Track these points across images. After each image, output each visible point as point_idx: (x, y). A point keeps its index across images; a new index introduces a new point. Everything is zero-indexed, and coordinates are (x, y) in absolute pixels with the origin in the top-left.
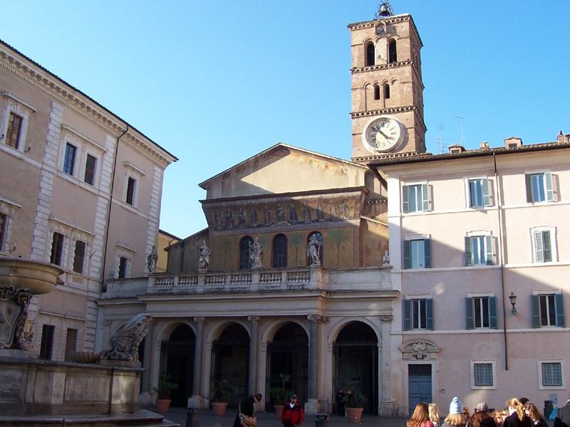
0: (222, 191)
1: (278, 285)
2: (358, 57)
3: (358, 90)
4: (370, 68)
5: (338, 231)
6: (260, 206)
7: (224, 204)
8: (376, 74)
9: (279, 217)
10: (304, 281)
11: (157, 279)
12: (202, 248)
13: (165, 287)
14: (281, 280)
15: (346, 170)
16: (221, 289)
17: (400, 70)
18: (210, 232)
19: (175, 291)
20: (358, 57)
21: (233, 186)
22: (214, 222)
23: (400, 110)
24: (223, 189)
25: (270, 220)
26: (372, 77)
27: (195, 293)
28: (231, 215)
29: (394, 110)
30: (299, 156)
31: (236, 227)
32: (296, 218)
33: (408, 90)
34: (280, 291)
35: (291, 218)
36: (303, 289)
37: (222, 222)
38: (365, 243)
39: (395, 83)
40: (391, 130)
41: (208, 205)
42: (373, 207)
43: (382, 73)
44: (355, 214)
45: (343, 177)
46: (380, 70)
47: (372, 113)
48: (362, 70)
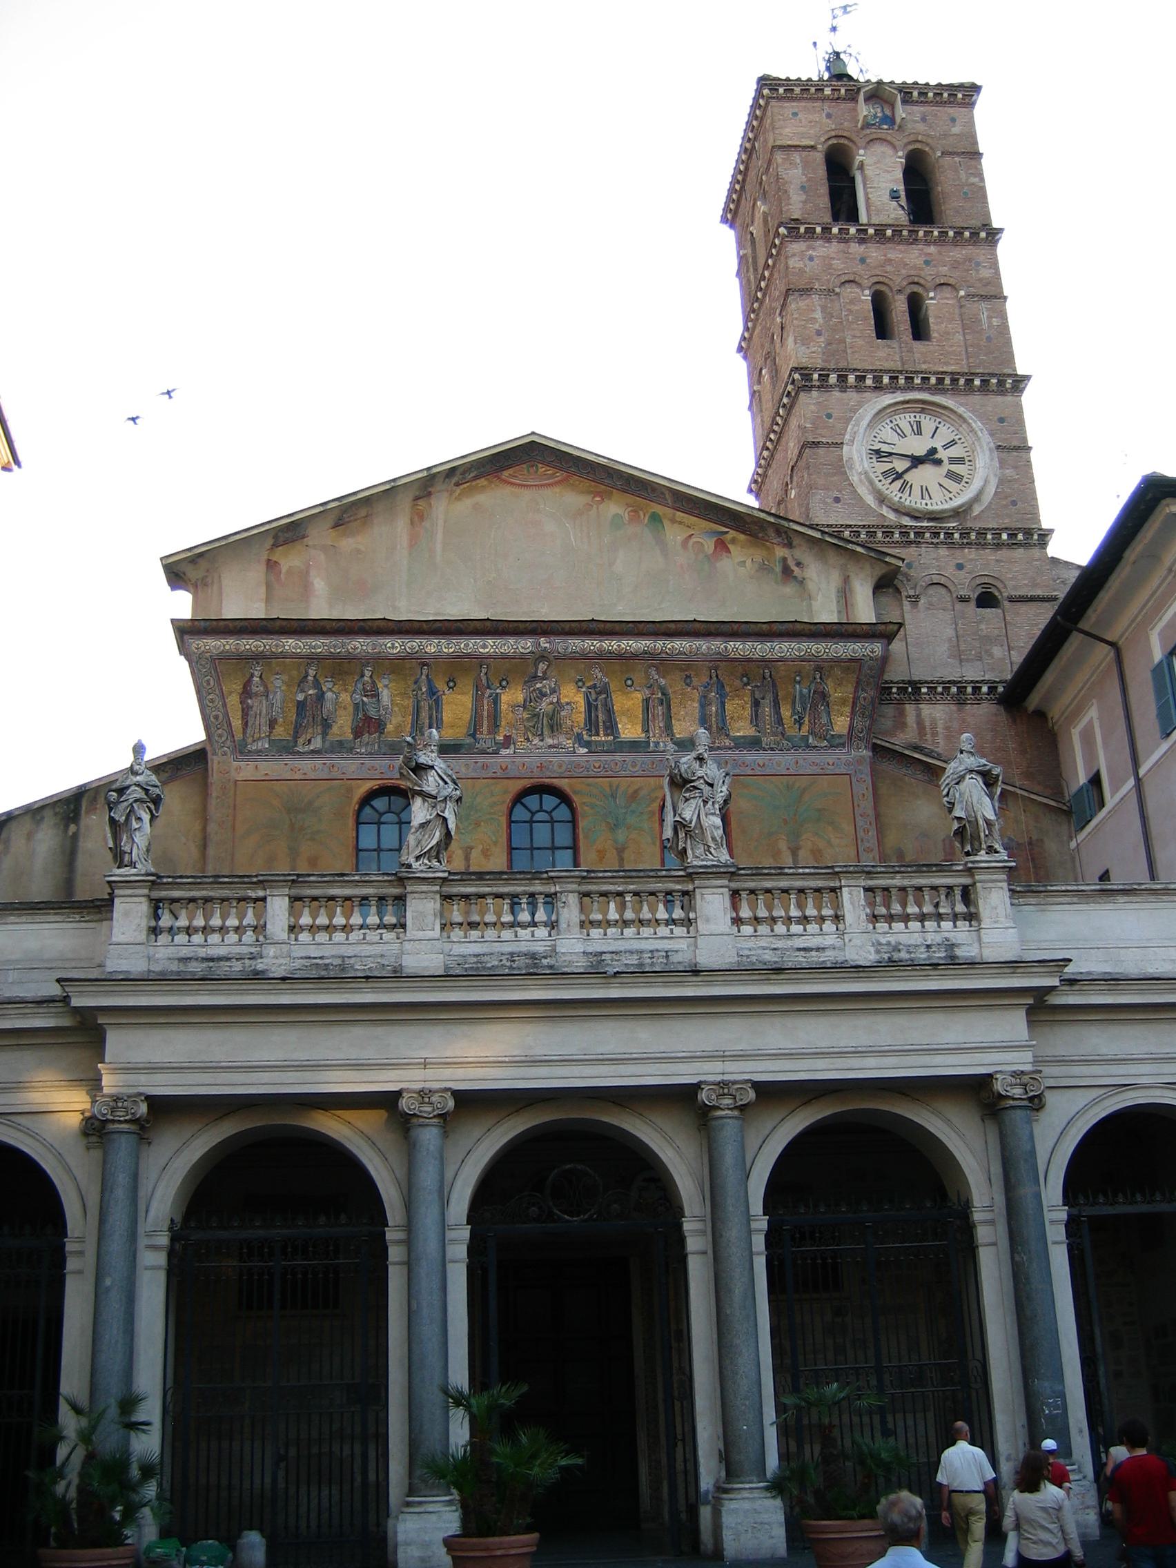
0: (268, 600)
1: (829, 941)
2: (803, 188)
3: (815, 297)
4: (853, 230)
5: (789, 787)
6: (457, 667)
7: (291, 644)
8: (874, 253)
9: (536, 715)
10: (947, 925)
11: (156, 906)
12: (423, 759)
13: (216, 946)
14: (837, 918)
15: (799, 564)
16: (533, 956)
17: (959, 253)
18: (215, 762)
19: (274, 961)
20: (803, 188)
21: (319, 585)
22: (237, 723)
23: (977, 382)
24: (269, 586)
25: (495, 726)
26: (863, 260)
27: (398, 976)
28: (321, 696)
29: (954, 381)
30: (604, 496)
31: (340, 746)
32: (611, 728)
33: (995, 322)
34: (858, 970)
35: (591, 725)
36: (953, 963)
37: (272, 723)
38: (892, 839)
39: (947, 292)
40: (946, 447)
41: (214, 644)
42: (910, 709)
43: (895, 253)
44: (851, 728)
45: (789, 589)
46: (890, 240)
47: (878, 379)
48: (827, 230)
